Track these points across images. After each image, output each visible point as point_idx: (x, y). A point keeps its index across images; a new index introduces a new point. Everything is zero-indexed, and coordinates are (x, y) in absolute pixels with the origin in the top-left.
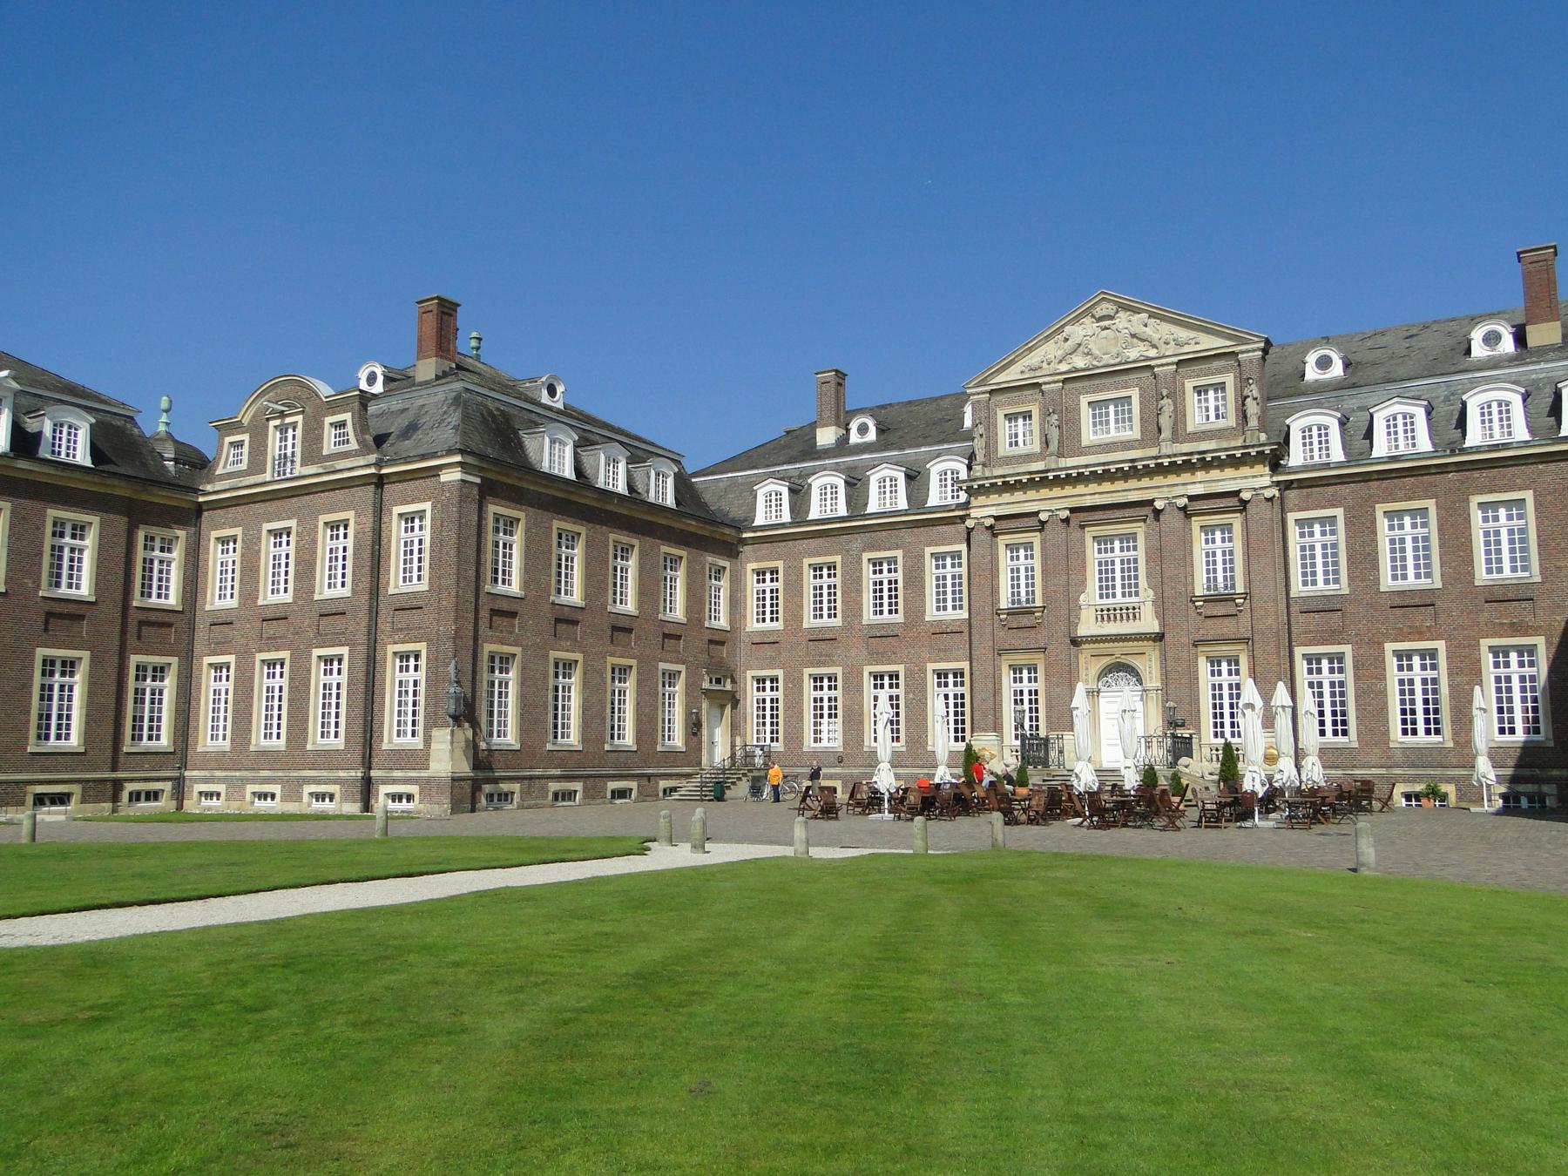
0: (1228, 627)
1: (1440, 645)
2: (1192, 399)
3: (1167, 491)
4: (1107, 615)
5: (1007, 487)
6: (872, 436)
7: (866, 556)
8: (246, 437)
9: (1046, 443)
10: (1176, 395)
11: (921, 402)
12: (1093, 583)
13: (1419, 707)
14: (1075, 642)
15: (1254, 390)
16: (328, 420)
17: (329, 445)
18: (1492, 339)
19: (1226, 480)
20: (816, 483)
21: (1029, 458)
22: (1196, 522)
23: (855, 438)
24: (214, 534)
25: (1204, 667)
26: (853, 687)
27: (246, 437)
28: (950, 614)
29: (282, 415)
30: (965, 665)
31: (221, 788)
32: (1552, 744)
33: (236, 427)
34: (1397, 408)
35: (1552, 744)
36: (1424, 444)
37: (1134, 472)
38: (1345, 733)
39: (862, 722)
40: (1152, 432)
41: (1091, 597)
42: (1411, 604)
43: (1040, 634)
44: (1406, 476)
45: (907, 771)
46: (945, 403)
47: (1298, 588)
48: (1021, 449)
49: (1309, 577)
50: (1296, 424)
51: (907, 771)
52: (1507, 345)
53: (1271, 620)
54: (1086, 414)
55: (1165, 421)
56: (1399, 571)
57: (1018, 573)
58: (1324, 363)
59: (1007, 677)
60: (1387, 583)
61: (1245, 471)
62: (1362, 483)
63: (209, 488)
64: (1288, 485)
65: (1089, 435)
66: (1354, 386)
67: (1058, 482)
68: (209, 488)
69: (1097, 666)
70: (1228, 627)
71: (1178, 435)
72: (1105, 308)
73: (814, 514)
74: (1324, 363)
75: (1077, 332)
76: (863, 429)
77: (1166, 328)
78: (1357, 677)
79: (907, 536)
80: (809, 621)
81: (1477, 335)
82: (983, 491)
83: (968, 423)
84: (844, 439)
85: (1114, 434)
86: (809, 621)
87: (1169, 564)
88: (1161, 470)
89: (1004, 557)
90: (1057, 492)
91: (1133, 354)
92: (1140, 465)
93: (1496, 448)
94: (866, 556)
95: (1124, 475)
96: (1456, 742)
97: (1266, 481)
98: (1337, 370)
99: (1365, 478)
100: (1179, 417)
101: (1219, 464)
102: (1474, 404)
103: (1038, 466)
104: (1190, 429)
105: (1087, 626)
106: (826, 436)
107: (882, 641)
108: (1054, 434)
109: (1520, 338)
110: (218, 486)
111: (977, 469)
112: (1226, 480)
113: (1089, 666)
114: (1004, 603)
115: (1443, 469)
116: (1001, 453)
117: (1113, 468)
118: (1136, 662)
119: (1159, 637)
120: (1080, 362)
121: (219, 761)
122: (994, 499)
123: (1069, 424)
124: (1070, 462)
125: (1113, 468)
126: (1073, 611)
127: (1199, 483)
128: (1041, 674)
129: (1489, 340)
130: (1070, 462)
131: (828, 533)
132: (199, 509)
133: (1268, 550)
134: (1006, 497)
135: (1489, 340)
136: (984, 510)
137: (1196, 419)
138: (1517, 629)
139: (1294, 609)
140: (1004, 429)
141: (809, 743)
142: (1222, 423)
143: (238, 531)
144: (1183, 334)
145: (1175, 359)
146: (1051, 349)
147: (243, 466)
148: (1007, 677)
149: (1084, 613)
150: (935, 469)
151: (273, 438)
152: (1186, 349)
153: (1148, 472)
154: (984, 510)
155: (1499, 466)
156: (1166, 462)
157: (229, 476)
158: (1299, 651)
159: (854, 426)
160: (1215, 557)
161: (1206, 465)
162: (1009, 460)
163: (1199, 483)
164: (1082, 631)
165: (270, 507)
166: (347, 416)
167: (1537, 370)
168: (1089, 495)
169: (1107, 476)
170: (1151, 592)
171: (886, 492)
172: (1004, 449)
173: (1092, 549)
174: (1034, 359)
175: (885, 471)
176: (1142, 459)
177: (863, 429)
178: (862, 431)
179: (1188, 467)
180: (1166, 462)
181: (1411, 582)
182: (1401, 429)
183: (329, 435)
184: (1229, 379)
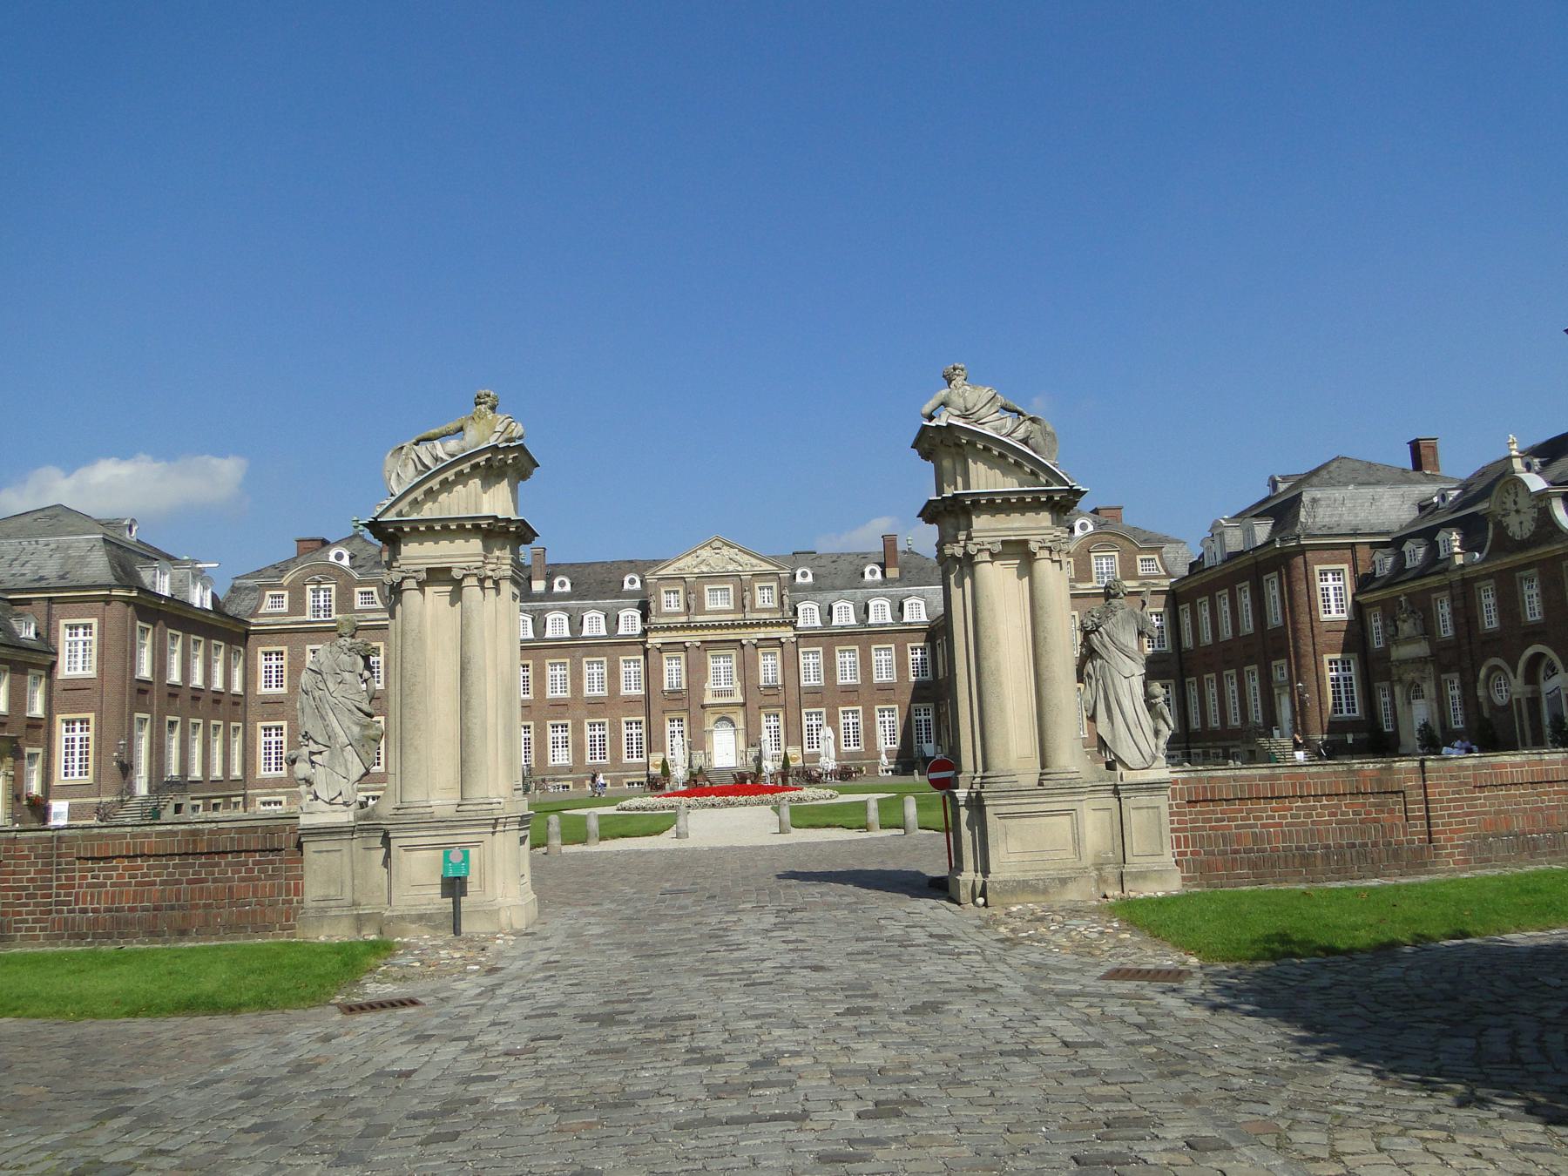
0: (774, 700)
2: (757, 591)
3: (748, 636)
4: (717, 694)
5: (669, 629)
6: (568, 588)
7: (585, 660)
8: (286, 593)
9: (688, 607)
10: (752, 590)
11: (580, 565)
12: (711, 679)
14: (703, 707)
15: (786, 592)
16: (357, 590)
17: (358, 605)
18: (873, 572)
19: (774, 632)
20: (550, 617)
21: (678, 614)
22: (760, 651)
23: (557, 588)
24: (260, 649)
25: (763, 718)
26: (578, 730)
27: (286, 593)
28: (633, 692)
29: (319, 583)
30: (643, 719)
31: (283, 799)
33: (281, 587)
34: (842, 604)
36: (853, 621)
37: (733, 626)
40: (741, 606)
41: (710, 685)
42: (849, 690)
43: (688, 704)
44: (846, 635)
46: (598, 568)
47: (803, 683)
48: (674, 609)
49: (807, 678)
50: (801, 607)
52: (878, 576)
53: (795, 697)
54: (707, 593)
55: (747, 602)
56: (844, 677)
57: (673, 672)
58: (804, 575)
59: (668, 723)
60: (840, 682)
62: (828, 638)
63: (253, 621)
64: (799, 636)
65: (708, 607)
66: (820, 589)
67: (696, 628)
68: (253, 621)
69: (713, 718)
70: (774, 700)
71: (754, 610)
72: (717, 544)
73: (549, 634)
74: (804, 575)
75: (705, 553)
76: (562, 584)
77: (746, 557)
79: (609, 650)
80: (549, 695)
81: (867, 570)
82: (656, 629)
83: (627, 586)
84: (550, 587)
85: (721, 606)
86: (549, 695)
87: (747, 670)
88: (746, 626)
89: (665, 662)
91: (731, 568)
93: (881, 625)
94: (585, 660)
95: (727, 627)
98: (810, 579)
99: (831, 635)
100: (753, 601)
101: (772, 625)
102: (872, 604)
103: (683, 619)
105: (709, 699)
106: (538, 586)
108: (693, 604)
109: (883, 574)
110: (261, 620)
111: (653, 619)
112: (774, 632)
113: (710, 719)
114: (666, 688)
115: (861, 633)
118: (733, 717)
119: (744, 705)
120: (705, 569)
121: (278, 782)
122: (661, 634)
123: (700, 598)
124: (699, 618)
127: (762, 633)
128: (685, 722)
129: (872, 574)
130: (699, 618)
131: (559, 646)
132: (247, 634)
133: (791, 665)
134: (668, 633)
135: (872, 574)
136: (655, 640)
137: (759, 604)
138: (888, 702)
140: (664, 597)
141: (551, 763)
142: (771, 605)
143: (285, 649)
144: (754, 561)
146: (689, 561)
147: (285, 609)
148: (668, 723)
150: (622, 614)
151: (309, 595)
153: (739, 626)
154: (655, 640)
155: (881, 634)
157: (271, 615)
159: (556, 581)
160: (769, 667)
161: (765, 625)
162: (668, 614)
163: (762, 633)
164: (706, 701)
165: (312, 636)
166: (374, 589)
167: (893, 590)
169: (720, 627)
171: (594, 625)
172: (665, 609)
173: (710, 660)
174: (680, 564)
175: (593, 613)
177: (562, 584)
178: (563, 585)
179: (758, 625)
181: (849, 681)
182: (845, 615)
183: (358, 598)
184: (775, 585)
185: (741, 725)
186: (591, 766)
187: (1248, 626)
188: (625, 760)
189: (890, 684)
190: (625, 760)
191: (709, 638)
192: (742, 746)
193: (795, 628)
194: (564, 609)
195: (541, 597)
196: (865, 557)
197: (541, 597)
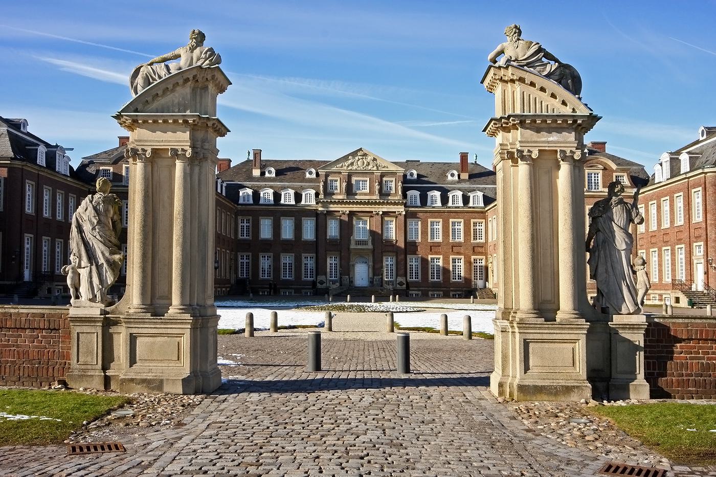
1: (441, 257)
4: (359, 242)
13: (435, 272)
14: (349, 249)
23: (267, 175)
30: (314, 255)
32: (464, 282)
35: (464, 282)
38: (418, 278)
39: (280, 271)
45: (295, 287)
51: (295, 287)
52: (456, 178)
61: (399, 206)
78: (422, 264)
84: (263, 174)
90: (347, 206)
92: (370, 201)
96: (444, 282)
97: (403, 210)
104: (383, 192)
107: (287, 246)
109: (459, 176)
114: (328, 238)
115: (444, 212)
116: (328, 191)
117: (363, 201)
119: (373, 251)
120: (355, 167)
125: (363, 201)
126: (349, 240)
138: (459, 253)
139: (408, 245)
145: (381, 172)
149: (352, 242)
152: (383, 169)
156: (378, 201)
158: (408, 256)
168: (355, 208)
170: (371, 237)
176: (371, 200)
178: (271, 173)
180: (378, 201)
185: (371, 264)
186: (283, 280)
187: (680, 221)
188: (304, 278)
189: (460, 243)
190: (304, 278)
191: (355, 209)
192: (371, 275)
193: (406, 206)
194: (271, 187)
195: (257, 179)
196: (449, 166)
197: (257, 179)
